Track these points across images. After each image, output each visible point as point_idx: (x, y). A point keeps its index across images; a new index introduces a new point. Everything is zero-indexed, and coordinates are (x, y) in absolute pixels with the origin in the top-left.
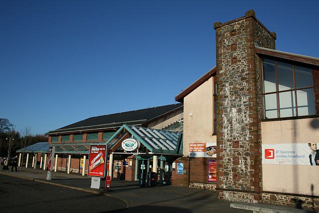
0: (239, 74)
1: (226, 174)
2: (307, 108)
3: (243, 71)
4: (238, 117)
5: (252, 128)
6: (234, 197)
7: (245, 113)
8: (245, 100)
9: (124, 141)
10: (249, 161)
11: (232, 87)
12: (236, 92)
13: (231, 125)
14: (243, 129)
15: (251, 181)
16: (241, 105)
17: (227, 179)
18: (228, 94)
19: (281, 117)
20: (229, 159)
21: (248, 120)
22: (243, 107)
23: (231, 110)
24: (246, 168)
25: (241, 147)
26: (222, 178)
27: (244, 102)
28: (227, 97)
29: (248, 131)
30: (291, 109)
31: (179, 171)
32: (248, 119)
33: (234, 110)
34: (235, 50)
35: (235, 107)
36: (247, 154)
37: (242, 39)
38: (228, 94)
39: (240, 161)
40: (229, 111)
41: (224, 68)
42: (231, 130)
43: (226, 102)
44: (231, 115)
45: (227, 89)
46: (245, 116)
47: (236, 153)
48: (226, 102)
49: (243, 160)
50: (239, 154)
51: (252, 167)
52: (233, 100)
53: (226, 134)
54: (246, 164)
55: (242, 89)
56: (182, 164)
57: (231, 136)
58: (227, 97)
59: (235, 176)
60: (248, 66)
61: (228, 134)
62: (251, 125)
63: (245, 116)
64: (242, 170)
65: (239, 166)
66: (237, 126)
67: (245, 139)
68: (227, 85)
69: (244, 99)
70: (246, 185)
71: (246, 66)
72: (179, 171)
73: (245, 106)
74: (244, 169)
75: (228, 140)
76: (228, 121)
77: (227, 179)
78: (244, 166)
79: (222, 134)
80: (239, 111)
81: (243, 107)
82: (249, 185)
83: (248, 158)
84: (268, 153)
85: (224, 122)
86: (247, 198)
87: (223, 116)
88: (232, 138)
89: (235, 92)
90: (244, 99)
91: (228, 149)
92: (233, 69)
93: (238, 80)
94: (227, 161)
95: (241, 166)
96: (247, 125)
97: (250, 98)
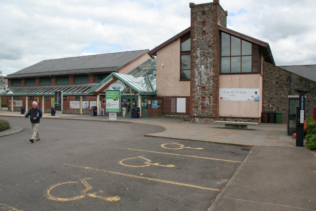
0: (207, 43)
1: (197, 107)
2: (251, 56)
3: (209, 41)
4: (205, 71)
5: (215, 79)
6: (202, 121)
7: (210, 69)
8: (210, 61)
9: (111, 85)
10: (212, 99)
11: (202, 51)
12: (204, 55)
13: (201, 76)
14: (208, 79)
15: (213, 111)
16: (207, 64)
17: (197, 110)
18: (199, 55)
19: (231, 72)
20: (199, 98)
21: (212, 74)
22: (209, 65)
23: (201, 66)
24: (210, 103)
25: (207, 90)
26: (194, 109)
27: (210, 62)
28: (198, 57)
29: (212, 81)
30: (242, 55)
31: (154, 106)
32: (212, 73)
33: (203, 67)
34: (205, 25)
35: (203, 64)
36: (211, 95)
37: (210, 19)
38: (199, 55)
39: (206, 99)
40: (199, 67)
41: (196, 37)
42: (201, 80)
43: (197, 61)
44: (200, 70)
45: (198, 52)
46: (210, 71)
47: (204, 94)
48: (197, 61)
49: (208, 98)
50: (206, 95)
51: (213, 102)
52: (202, 60)
53: (197, 82)
54: (210, 101)
55: (209, 53)
56: (156, 102)
57: (200, 83)
58: (198, 57)
59: (202, 108)
60: (214, 38)
61: (198, 82)
62: (214, 77)
63: (210, 71)
64: (207, 104)
65: (206, 102)
66: (205, 77)
67: (210, 86)
68: (198, 49)
69: (210, 60)
70: (209, 113)
71: (212, 38)
72: (154, 106)
73: (210, 64)
74: (208, 104)
75: (198, 86)
76: (198, 74)
77: (197, 110)
78: (208, 102)
79: (194, 82)
80: (206, 67)
81: (209, 65)
82: (211, 113)
83: (211, 97)
84: (221, 98)
85: (196, 74)
86: (210, 121)
87: (195, 70)
88: (201, 84)
89: (203, 55)
90: (210, 60)
91: (199, 93)
92: (203, 39)
93: (206, 47)
94: (197, 99)
95: (207, 102)
96: (211, 77)
97: (213, 60)
